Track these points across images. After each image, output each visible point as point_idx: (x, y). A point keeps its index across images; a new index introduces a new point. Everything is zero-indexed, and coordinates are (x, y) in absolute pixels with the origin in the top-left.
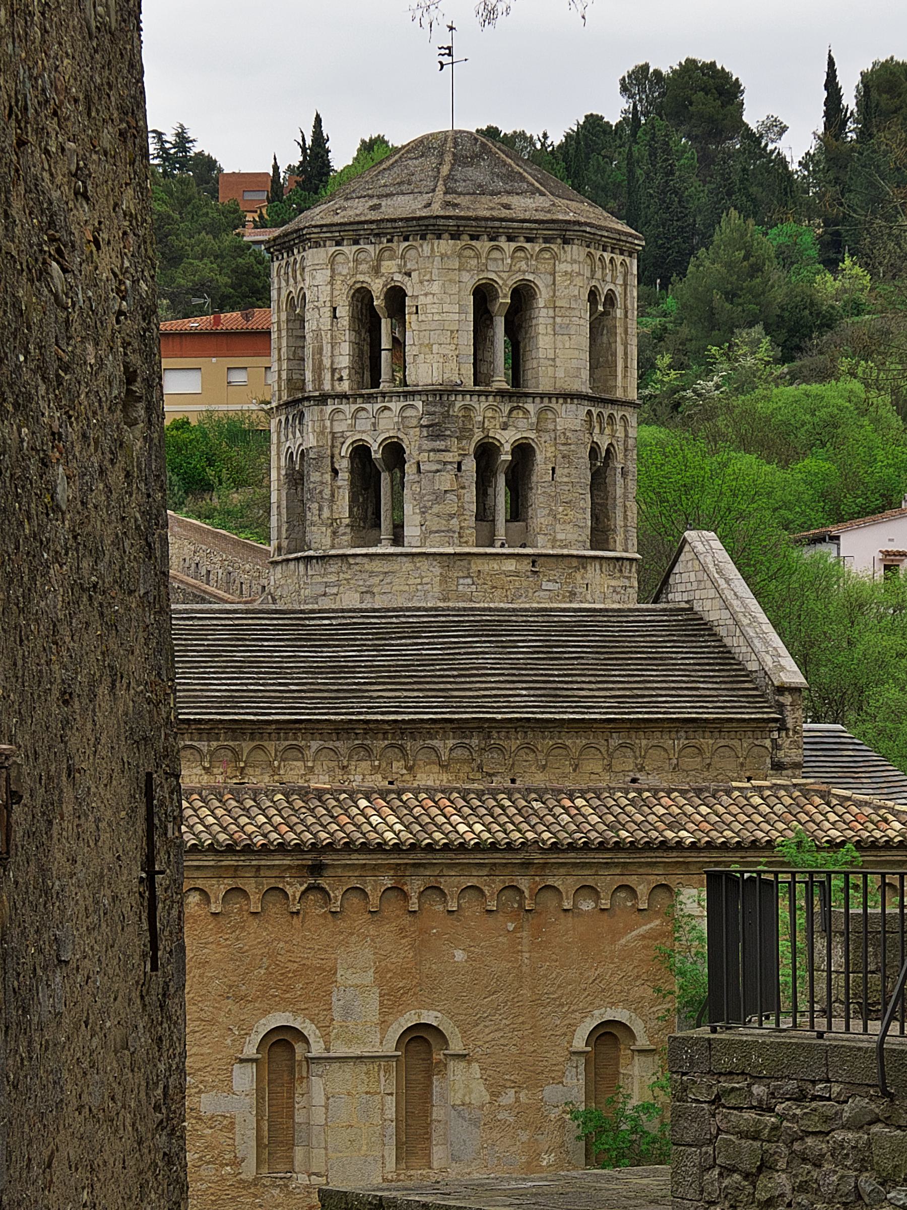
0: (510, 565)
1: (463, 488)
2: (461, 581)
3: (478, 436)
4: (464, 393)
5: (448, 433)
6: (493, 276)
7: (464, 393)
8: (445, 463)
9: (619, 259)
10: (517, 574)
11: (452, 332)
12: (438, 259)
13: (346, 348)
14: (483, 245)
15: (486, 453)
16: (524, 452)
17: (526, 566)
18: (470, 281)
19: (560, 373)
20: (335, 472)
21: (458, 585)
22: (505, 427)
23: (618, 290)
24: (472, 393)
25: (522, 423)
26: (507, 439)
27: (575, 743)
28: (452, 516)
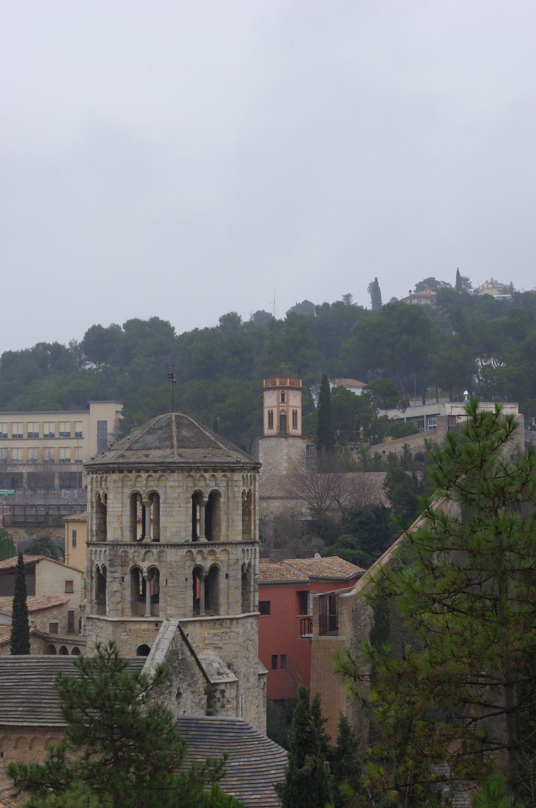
0: (145, 626)
1: (124, 589)
2: (122, 634)
3: (131, 564)
4: (124, 545)
5: (116, 564)
6: (138, 489)
7: (124, 545)
8: (115, 578)
9: (219, 475)
10: (148, 630)
11: (118, 516)
12: (112, 483)
13: (94, 522)
14: (134, 475)
15: (136, 571)
16: (154, 572)
17: (152, 627)
18: (128, 491)
19: (168, 535)
20: (92, 578)
21: (121, 635)
22: (143, 560)
23: (222, 490)
24: (127, 545)
25: (152, 558)
26: (145, 566)
27: (29, 736)
28: (118, 603)
